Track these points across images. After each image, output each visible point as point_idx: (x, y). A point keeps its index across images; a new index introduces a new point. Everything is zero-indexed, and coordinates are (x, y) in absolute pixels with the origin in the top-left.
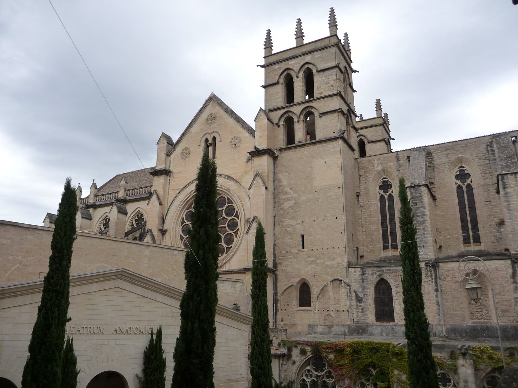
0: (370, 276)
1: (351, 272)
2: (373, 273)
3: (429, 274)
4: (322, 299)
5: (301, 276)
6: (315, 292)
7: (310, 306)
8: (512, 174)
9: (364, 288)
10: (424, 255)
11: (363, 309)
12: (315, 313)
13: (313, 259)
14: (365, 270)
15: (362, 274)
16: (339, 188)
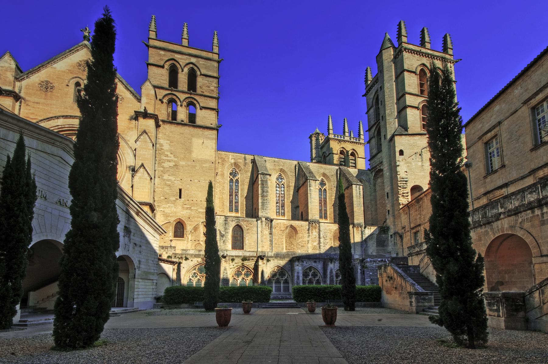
0: (231, 222)
1: (217, 218)
2: (233, 221)
3: (267, 225)
4: (194, 233)
5: (178, 217)
6: (189, 228)
7: (183, 237)
8: (314, 180)
9: (226, 229)
10: (265, 214)
11: (224, 241)
12: (188, 242)
13: (188, 206)
14: (227, 218)
15: (225, 220)
16: (213, 163)
